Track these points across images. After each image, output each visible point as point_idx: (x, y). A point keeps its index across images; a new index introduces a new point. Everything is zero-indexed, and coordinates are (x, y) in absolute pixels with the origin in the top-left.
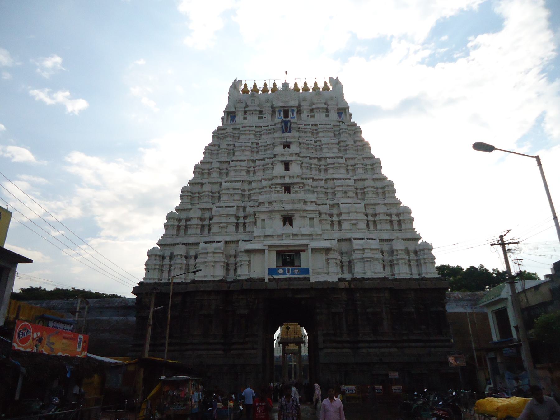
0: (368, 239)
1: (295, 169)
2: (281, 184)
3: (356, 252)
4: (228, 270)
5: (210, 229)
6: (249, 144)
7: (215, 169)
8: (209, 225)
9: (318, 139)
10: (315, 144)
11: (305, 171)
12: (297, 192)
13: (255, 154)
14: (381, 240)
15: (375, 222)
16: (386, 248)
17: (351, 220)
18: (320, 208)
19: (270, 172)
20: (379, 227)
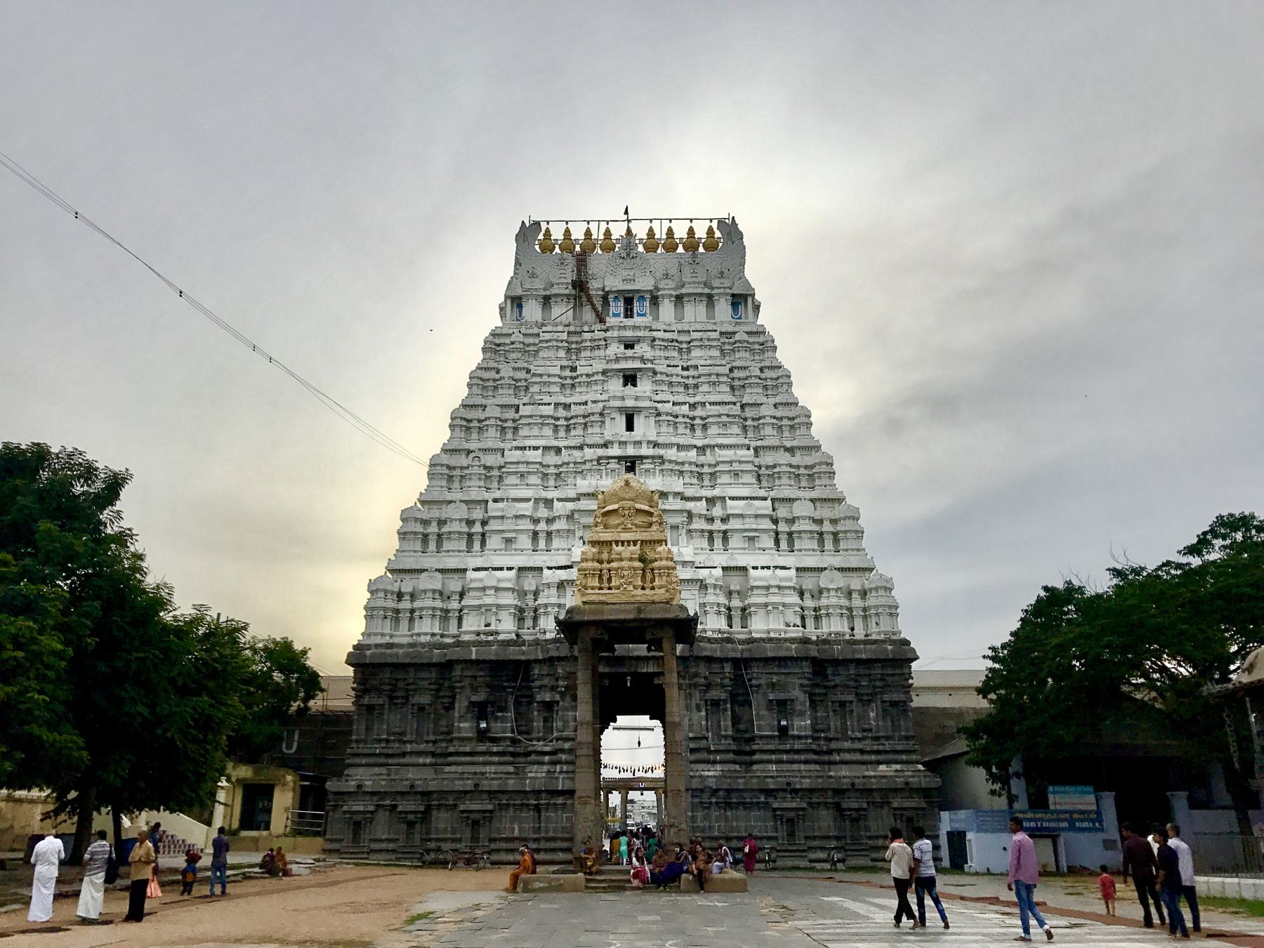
0: (776, 567)
2: (620, 458)
3: (755, 592)
4: (521, 620)
5: (483, 543)
6: (557, 371)
7: (492, 422)
8: (483, 535)
10: (685, 373)
11: (664, 429)
12: (647, 471)
13: (568, 391)
14: (798, 569)
15: (790, 534)
17: (746, 530)
18: (690, 505)
19: (597, 430)
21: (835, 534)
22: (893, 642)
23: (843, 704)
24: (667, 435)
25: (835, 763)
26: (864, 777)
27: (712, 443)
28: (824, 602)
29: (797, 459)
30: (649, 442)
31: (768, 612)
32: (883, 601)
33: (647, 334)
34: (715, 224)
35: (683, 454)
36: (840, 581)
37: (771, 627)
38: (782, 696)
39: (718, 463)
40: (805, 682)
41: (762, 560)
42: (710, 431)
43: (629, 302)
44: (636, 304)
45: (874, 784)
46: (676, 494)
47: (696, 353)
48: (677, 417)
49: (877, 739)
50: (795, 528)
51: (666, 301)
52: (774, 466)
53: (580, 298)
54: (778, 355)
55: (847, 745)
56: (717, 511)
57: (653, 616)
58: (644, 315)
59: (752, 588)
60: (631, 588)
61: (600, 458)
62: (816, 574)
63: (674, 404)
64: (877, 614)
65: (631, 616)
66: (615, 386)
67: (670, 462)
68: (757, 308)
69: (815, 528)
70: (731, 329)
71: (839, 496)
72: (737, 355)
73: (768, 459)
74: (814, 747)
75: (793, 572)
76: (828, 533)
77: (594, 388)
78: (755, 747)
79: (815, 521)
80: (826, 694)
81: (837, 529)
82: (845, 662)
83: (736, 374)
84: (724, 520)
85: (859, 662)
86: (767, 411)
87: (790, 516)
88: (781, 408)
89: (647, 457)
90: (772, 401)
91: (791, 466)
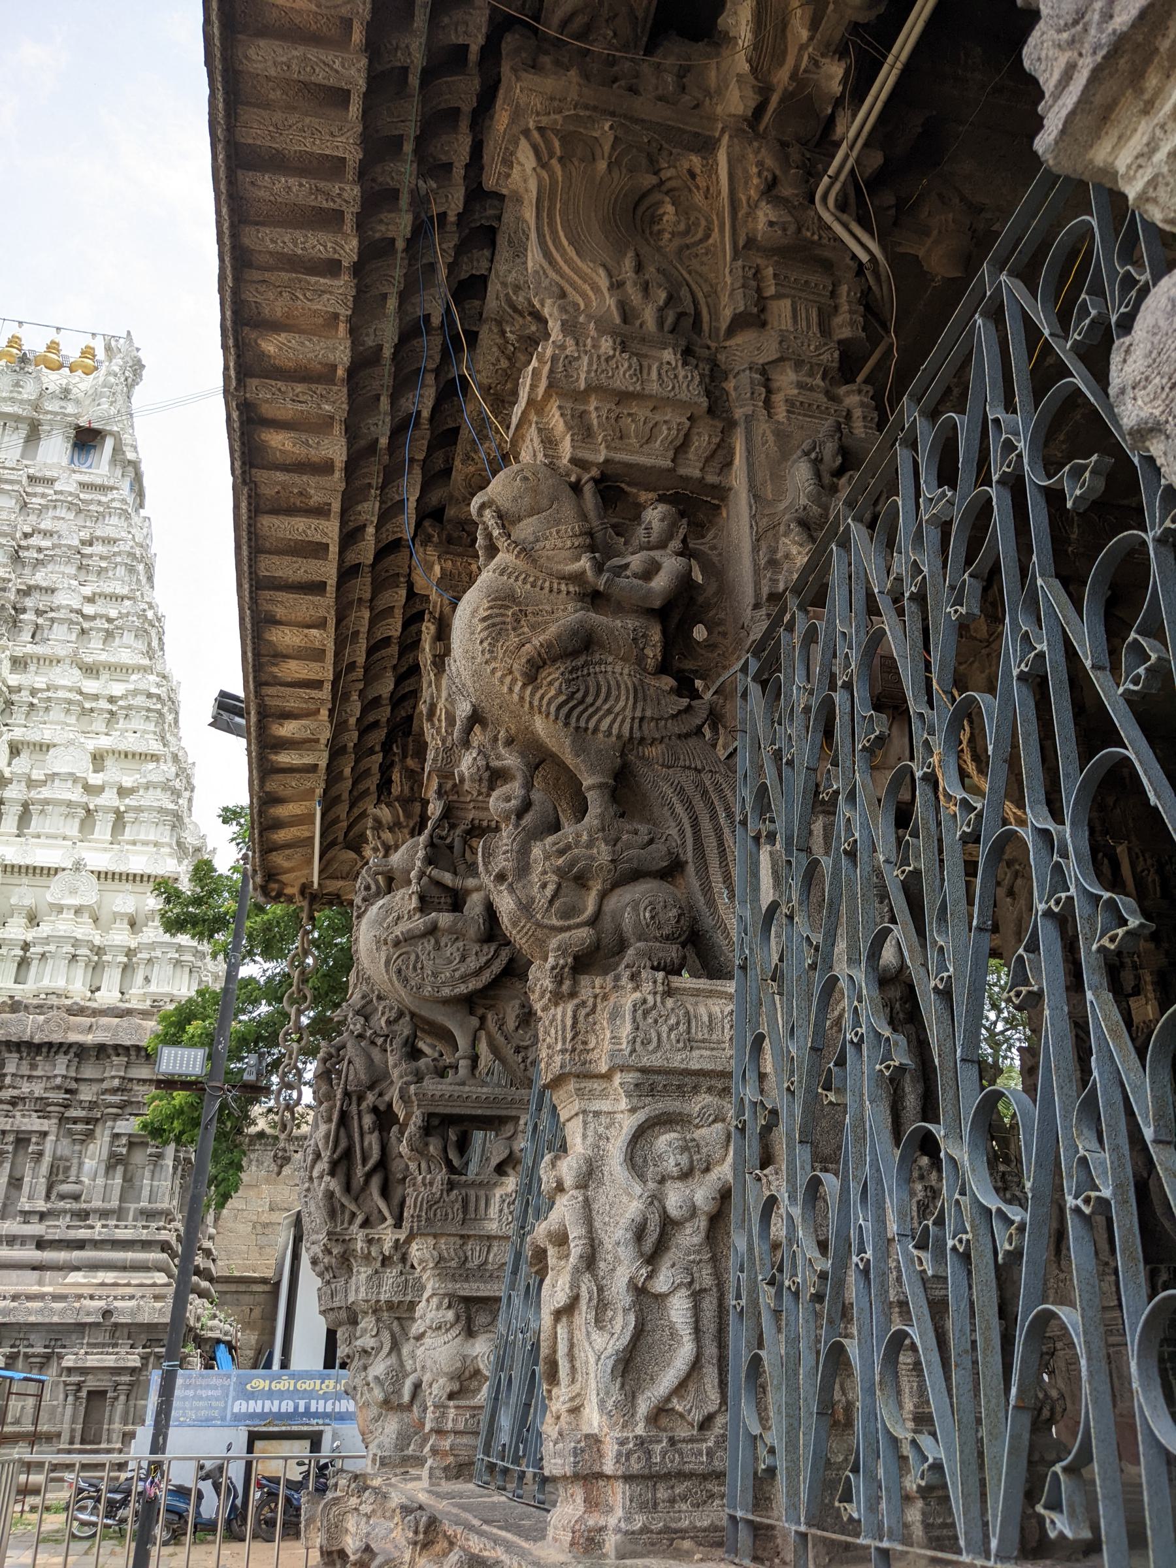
15: (26, 806)
20: (36, 825)
21: (119, 815)
26: (15, 1298)
28: (45, 929)
29: (90, 686)
36: (88, 893)
45: (32, 1313)
49: (83, 1215)
50: (45, 793)
72: (51, 513)
76: (106, 810)
82: (51, 1049)
83: (34, 541)
85: (81, 1052)
90: (87, 591)
91: (81, 693)
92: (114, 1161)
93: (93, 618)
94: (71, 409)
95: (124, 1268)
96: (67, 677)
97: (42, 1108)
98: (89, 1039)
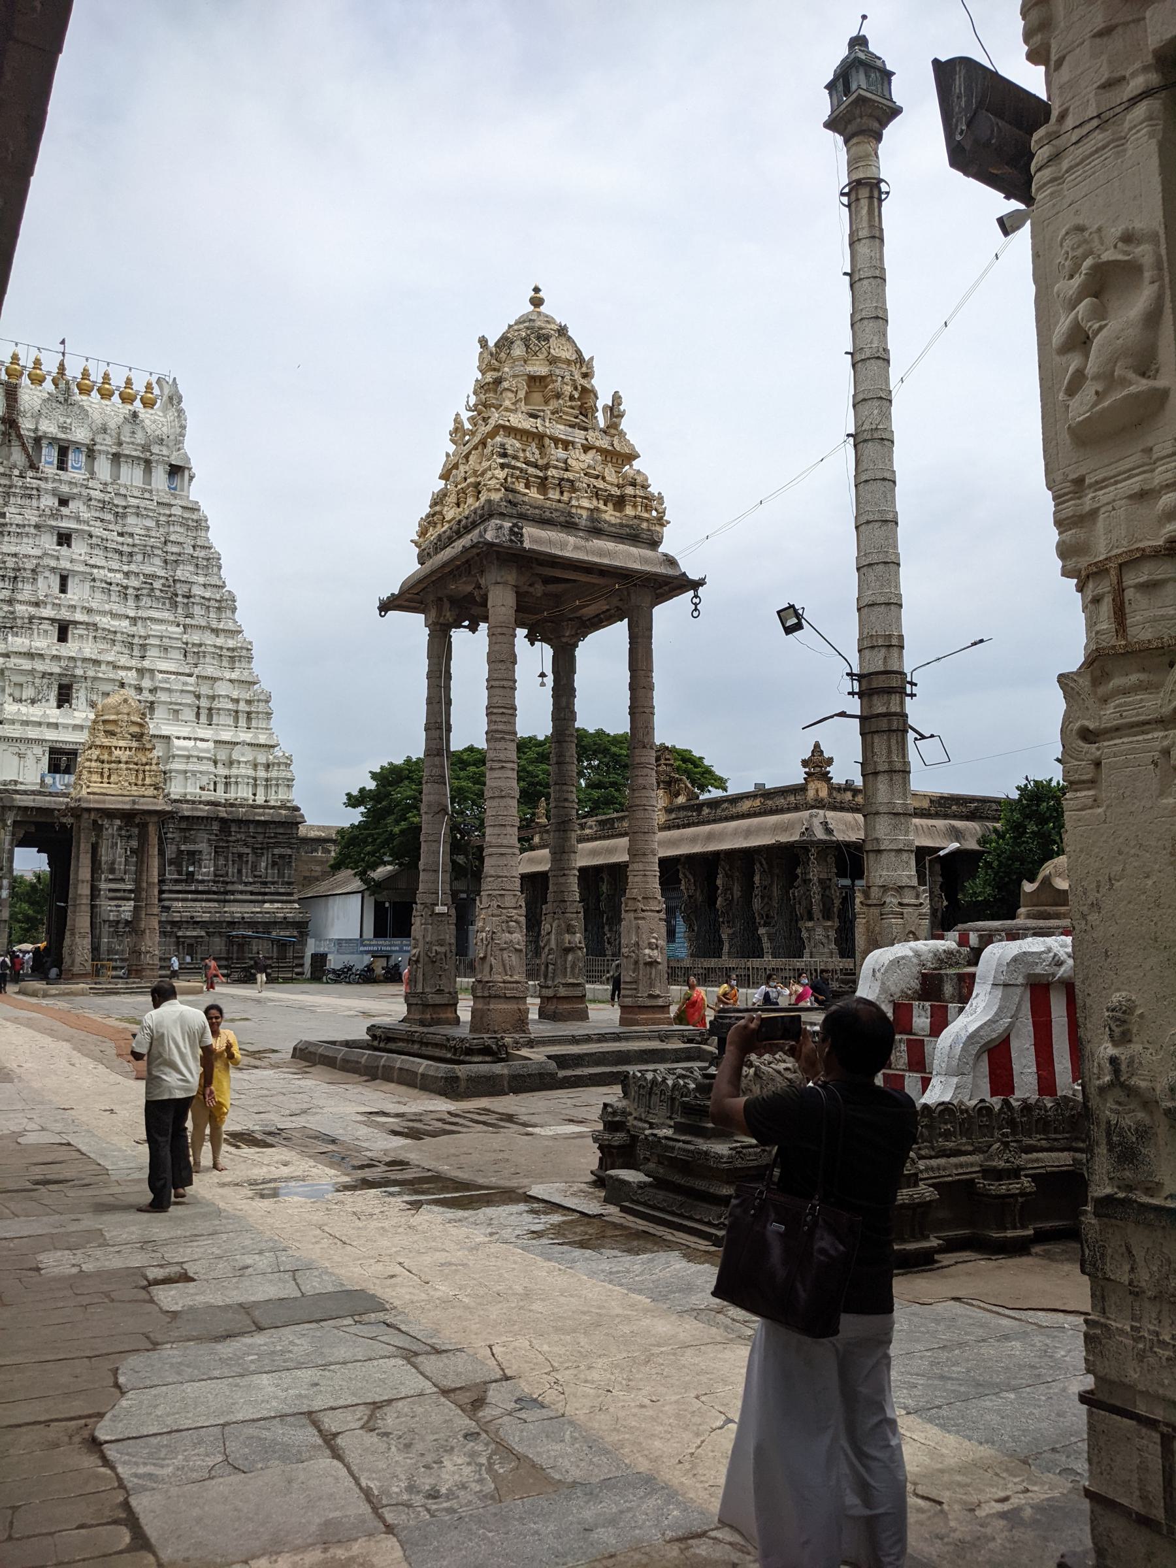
0: (196, 739)
1: (77, 592)
2: (53, 620)
9: (125, 529)
10: (120, 539)
11: (98, 595)
12: (81, 636)
14: (216, 742)
15: (210, 709)
16: (222, 755)
17: (171, 703)
18: (122, 673)
21: (249, 713)
22: (288, 808)
23: (240, 855)
24: (97, 601)
25: (229, 901)
27: (145, 615)
28: (234, 771)
29: (220, 641)
30: (83, 608)
31: (186, 778)
32: (283, 774)
33: (85, 492)
34: (154, 380)
35: (116, 623)
36: (247, 755)
37: (188, 790)
38: (192, 847)
39: (149, 636)
40: (214, 837)
41: (185, 731)
42: (142, 604)
43: (63, 452)
44: (71, 456)
46: (108, 663)
47: (131, 520)
48: (111, 584)
49: (265, 883)
51: (103, 457)
52: (200, 645)
53: (10, 435)
54: (210, 535)
55: (241, 887)
56: (146, 683)
57: (146, 808)
58: (79, 468)
59: (174, 756)
60: (126, 784)
61: (31, 618)
62: (230, 746)
63: (110, 570)
64: (277, 785)
65: (128, 807)
66: (48, 542)
67: (104, 629)
68: (191, 478)
69: (230, 706)
70: (164, 500)
71: (255, 680)
72: (172, 529)
73: (195, 638)
74: (214, 889)
75: (211, 745)
77: (25, 540)
78: (165, 888)
79: (232, 700)
80: (228, 847)
81: (254, 710)
84: (153, 691)
86: (197, 591)
87: (210, 693)
88: (209, 588)
89: (81, 623)
90: (201, 580)
91: (215, 646)
92: (274, 864)
93: (209, 600)
94: (165, 452)
95: (282, 902)
96: (209, 639)
97: (246, 845)
98: (263, 818)
